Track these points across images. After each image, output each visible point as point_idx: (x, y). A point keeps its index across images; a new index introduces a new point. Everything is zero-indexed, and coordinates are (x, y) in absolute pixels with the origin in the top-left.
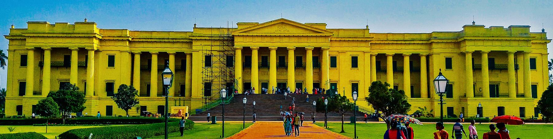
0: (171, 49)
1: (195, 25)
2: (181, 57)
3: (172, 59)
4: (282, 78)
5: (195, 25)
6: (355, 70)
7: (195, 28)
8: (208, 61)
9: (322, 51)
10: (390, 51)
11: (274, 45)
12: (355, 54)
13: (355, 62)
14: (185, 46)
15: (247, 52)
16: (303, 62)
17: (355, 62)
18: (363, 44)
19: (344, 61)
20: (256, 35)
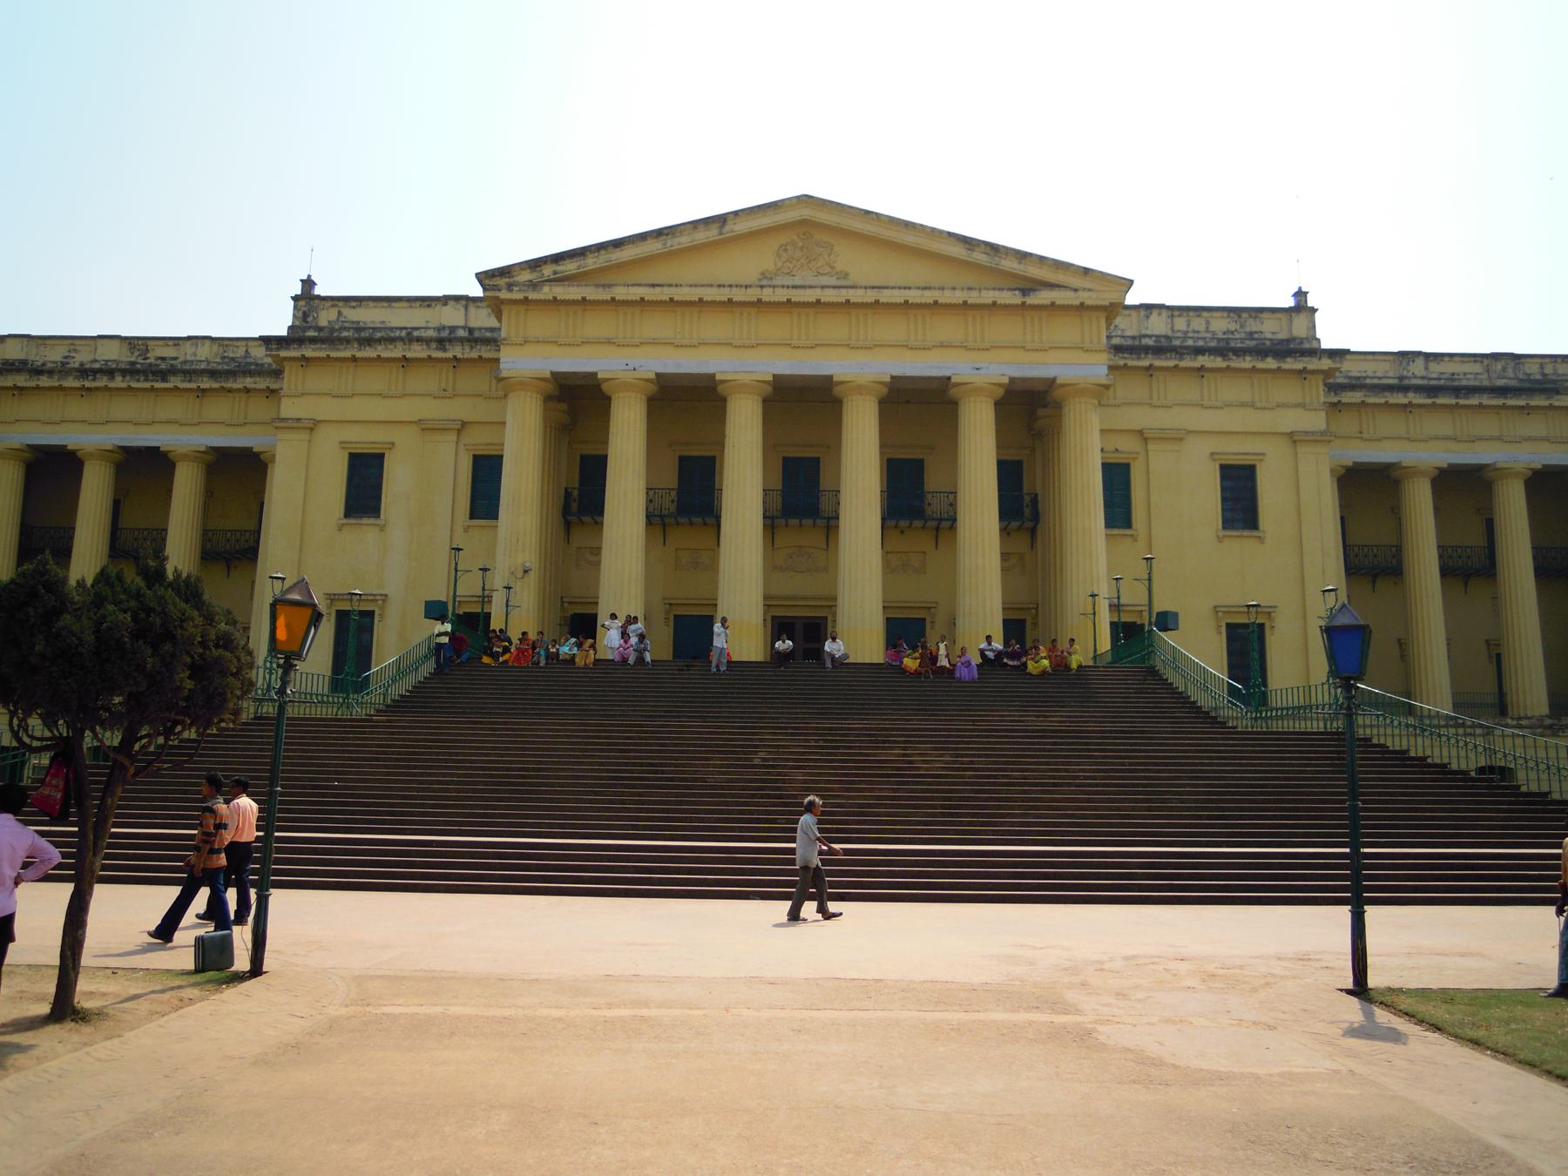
0: (185, 430)
1: (308, 283)
2: (239, 474)
3: (186, 486)
4: (800, 586)
5: (308, 283)
6: (1240, 545)
7: (307, 298)
8: (364, 486)
9: (1058, 406)
10: (1421, 446)
11: (745, 361)
12: (1237, 450)
13: (1240, 497)
14: (259, 409)
15: (577, 403)
16: (933, 481)
17: (1240, 497)
18: (1288, 391)
19: (1181, 493)
20: (636, 293)
